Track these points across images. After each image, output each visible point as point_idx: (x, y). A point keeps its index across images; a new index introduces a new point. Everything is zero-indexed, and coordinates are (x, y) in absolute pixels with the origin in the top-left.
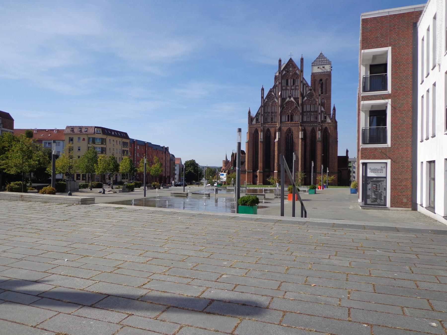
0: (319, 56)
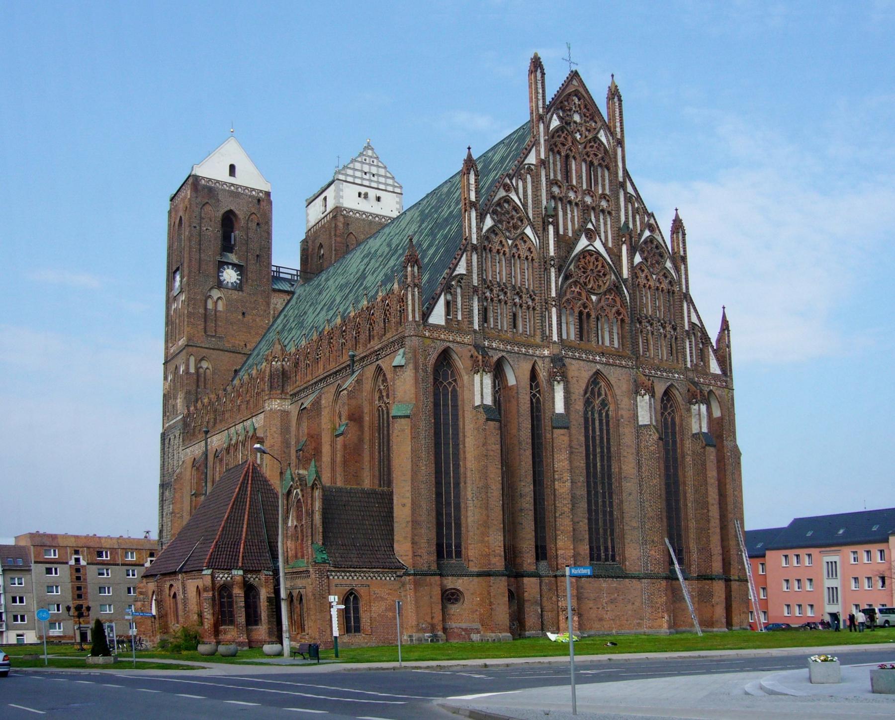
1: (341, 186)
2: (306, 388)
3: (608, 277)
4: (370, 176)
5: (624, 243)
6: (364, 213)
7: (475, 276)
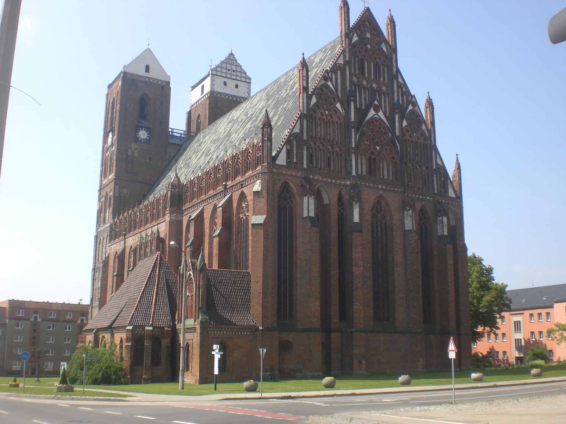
0: (227, 59)
1: (213, 78)
2: (194, 206)
3: (387, 135)
4: (231, 72)
5: (397, 113)
6: (227, 95)
7: (305, 134)
